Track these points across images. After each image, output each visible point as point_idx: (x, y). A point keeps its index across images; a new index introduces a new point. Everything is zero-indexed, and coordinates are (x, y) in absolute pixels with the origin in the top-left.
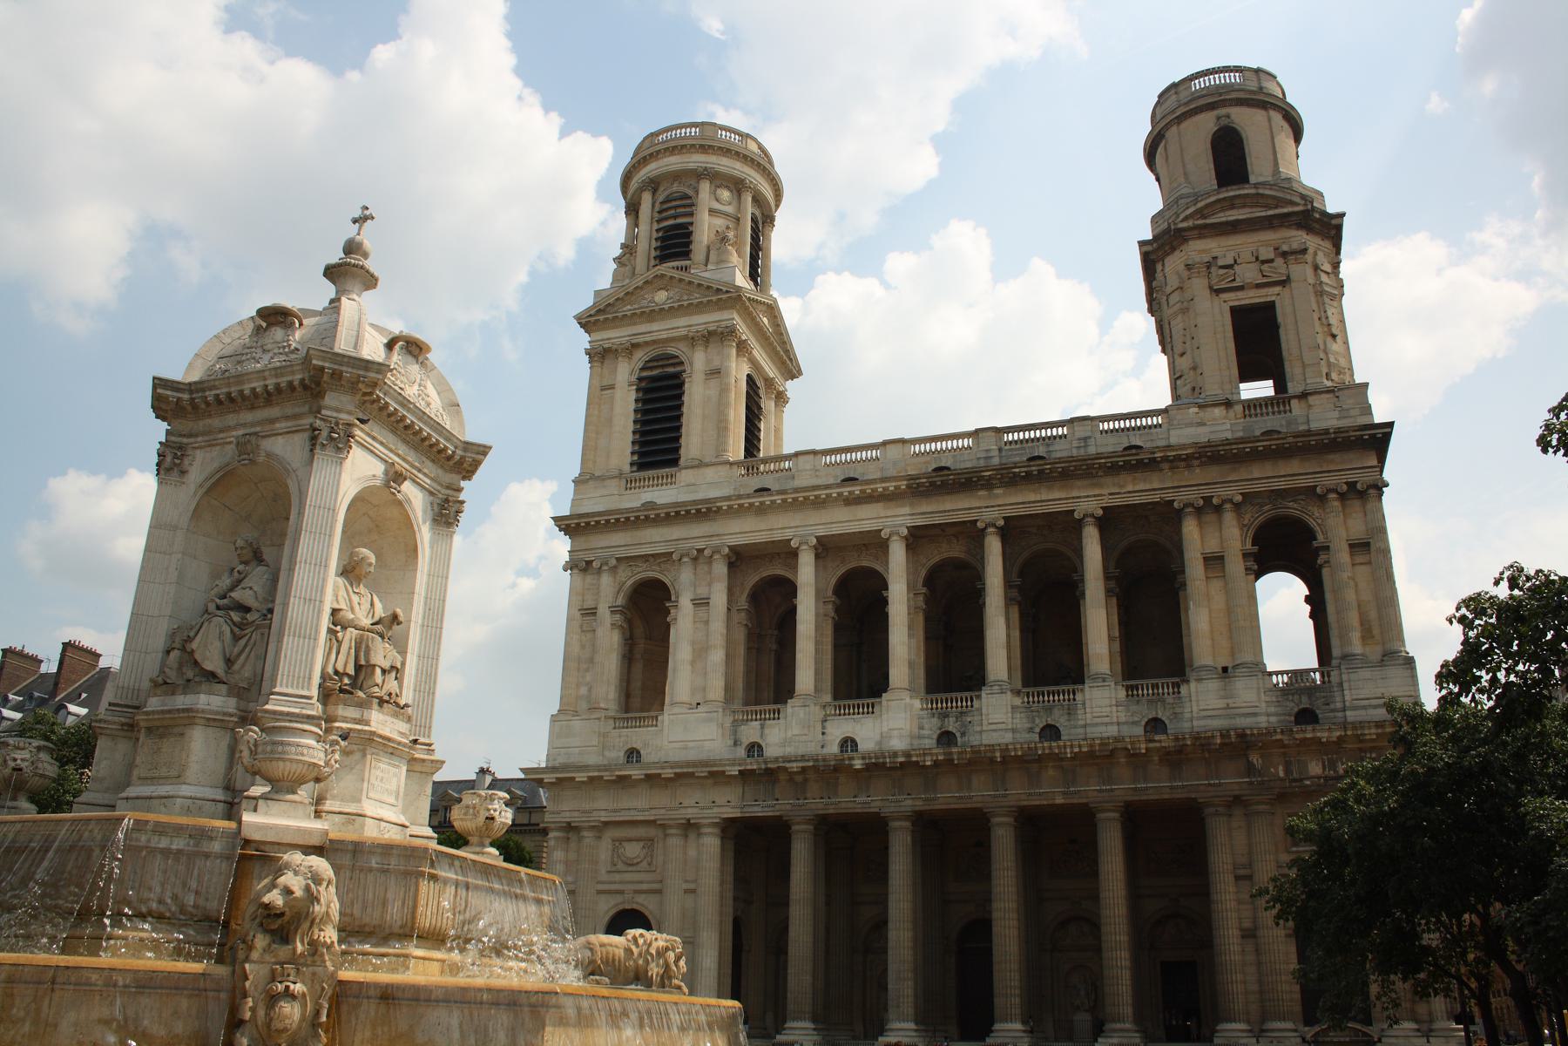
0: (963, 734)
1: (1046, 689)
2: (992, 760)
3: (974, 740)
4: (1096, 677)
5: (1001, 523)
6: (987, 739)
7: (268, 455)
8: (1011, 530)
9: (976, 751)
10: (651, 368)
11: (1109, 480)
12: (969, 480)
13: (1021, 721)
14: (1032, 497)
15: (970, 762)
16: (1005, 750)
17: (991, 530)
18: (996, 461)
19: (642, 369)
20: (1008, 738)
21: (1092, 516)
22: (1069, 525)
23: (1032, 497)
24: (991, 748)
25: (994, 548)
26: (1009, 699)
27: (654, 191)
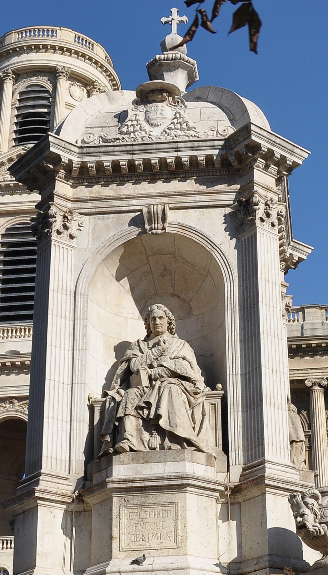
7: (182, 226)
10: (12, 236)
19: (3, 236)
27: (16, 81)
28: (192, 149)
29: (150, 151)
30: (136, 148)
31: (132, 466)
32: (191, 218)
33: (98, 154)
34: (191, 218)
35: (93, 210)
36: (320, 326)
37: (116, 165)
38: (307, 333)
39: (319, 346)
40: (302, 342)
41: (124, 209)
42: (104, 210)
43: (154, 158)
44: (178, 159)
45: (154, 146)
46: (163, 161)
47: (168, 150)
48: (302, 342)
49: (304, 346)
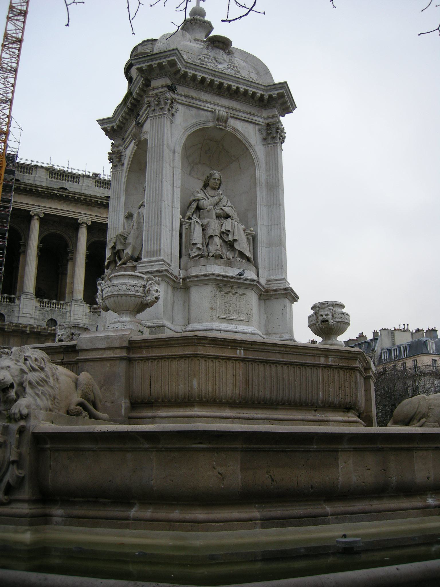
0: (9, 316)
1: (52, 301)
2: (23, 332)
3: (15, 320)
4: (77, 300)
5: (42, 215)
6: (22, 321)
7: (234, 129)
8: (46, 220)
9: (17, 325)
11: (96, 209)
12: (31, 190)
13: (36, 314)
14: (59, 207)
15: (14, 331)
16: (32, 327)
17: (36, 217)
18: (44, 184)
20: (31, 322)
21: (86, 224)
22: (74, 225)
23: (59, 207)
24: (26, 326)
25: (35, 226)
26: (34, 303)
28: (247, 85)
29: (224, 78)
30: (217, 73)
31: (223, 267)
32: (239, 125)
33: (195, 70)
34: (239, 125)
35: (185, 103)
36: (45, 180)
37: (203, 79)
38: (37, 183)
39: (43, 192)
40: (33, 188)
41: (203, 107)
42: (191, 104)
43: (226, 83)
44: (238, 88)
45: (227, 77)
46: (229, 86)
47: (234, 81)
48: (33, 188)
49: (28, 189)
